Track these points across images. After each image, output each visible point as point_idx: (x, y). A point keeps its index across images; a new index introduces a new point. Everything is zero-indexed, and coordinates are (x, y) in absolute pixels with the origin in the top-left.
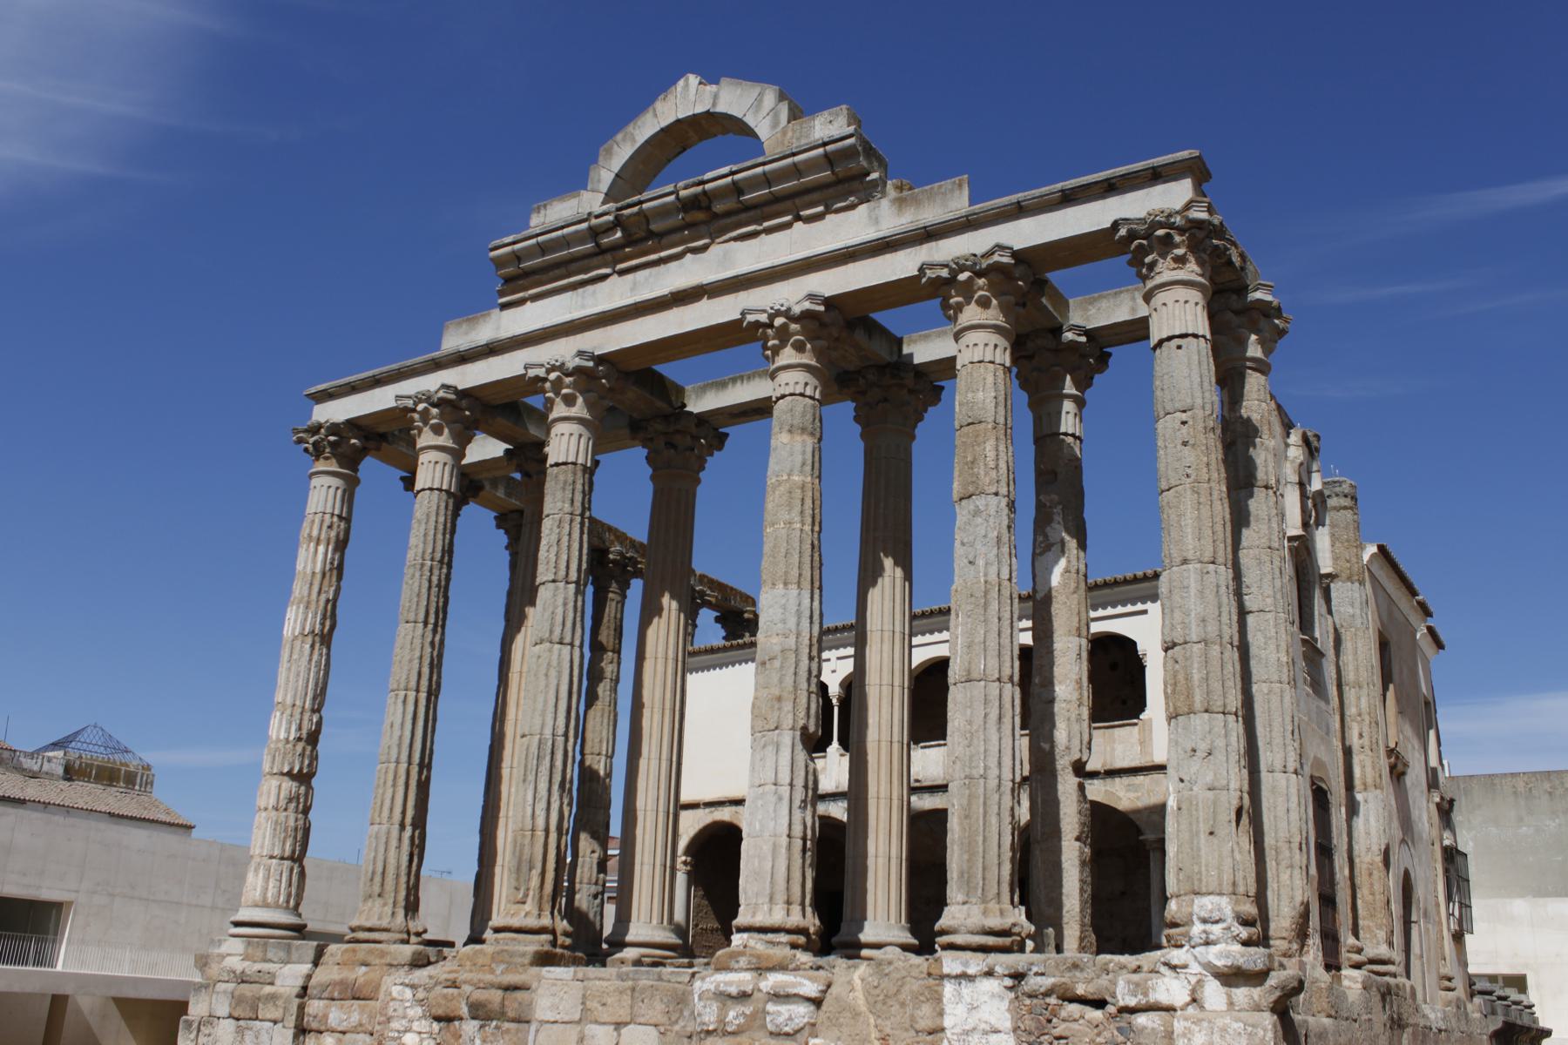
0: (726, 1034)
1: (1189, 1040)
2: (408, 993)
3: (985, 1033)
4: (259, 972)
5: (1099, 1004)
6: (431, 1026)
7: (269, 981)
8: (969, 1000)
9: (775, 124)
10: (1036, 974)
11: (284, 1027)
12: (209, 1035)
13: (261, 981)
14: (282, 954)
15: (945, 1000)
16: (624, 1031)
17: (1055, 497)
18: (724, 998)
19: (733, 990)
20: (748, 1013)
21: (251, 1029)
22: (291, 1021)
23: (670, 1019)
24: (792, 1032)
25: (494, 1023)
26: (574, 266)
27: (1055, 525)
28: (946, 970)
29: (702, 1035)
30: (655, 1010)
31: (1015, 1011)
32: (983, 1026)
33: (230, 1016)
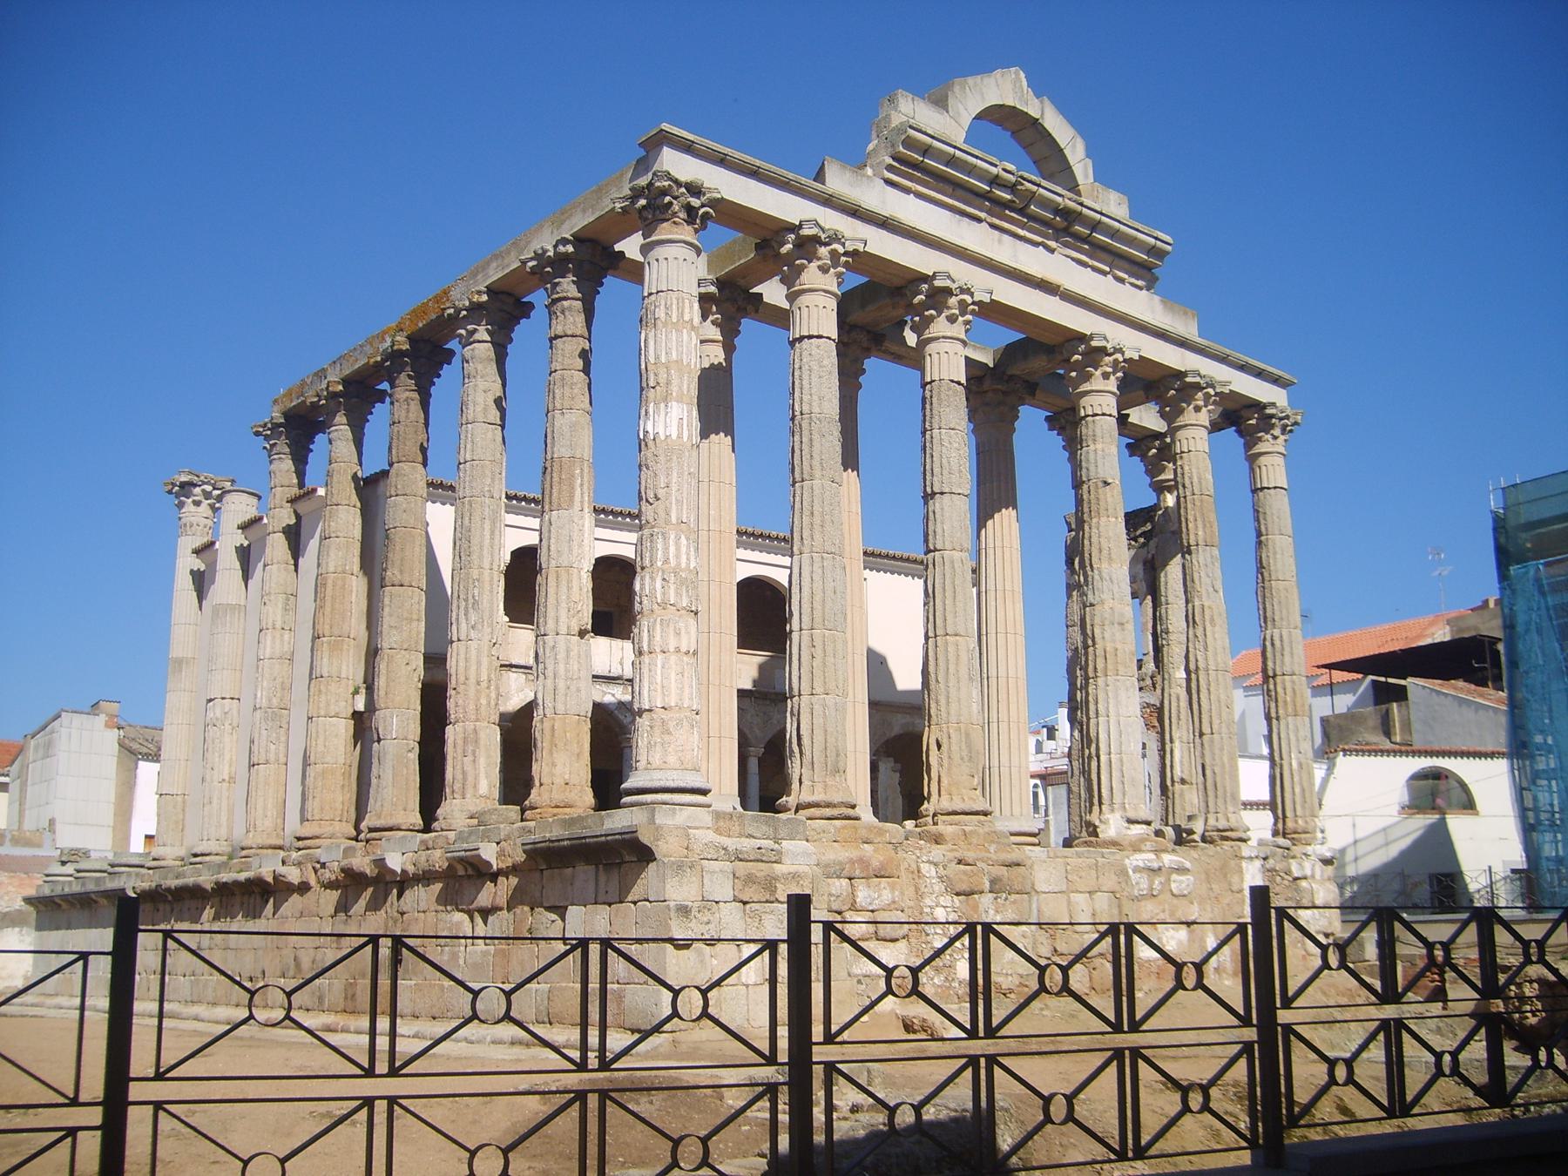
4: (759, 848)
6: (953, 901)
9: (1086, 176)
13: (764, 859)
14: (764, 828)
26: (960, 192)
28: (1244, 854)
30: (1109, 881)
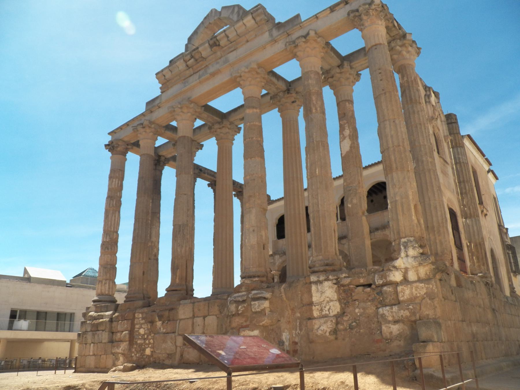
0: (239, 315)
1: (404, 293)
2: (140, 316)
3: (328, 302)
5: (369, 285)
6: (148, 326)
7: (101, 318)
8: (321, 290)
10: (345, 277)
11: (105, 332)
12: (86, 337)
15: (312, 291)
16: (206, 319)
17: (345, 121)
18: (238, 303)
19: (241, 299)
20: (245, 306)
21: (96, 334)
22: (107, 330)
23: (220, 312)
24: (260, 310)
25: (166, 322)
27: (346, 130)
28: (312, 280)
29: (231, 316)
31: (339, 293)
32: (328, 299)
33: (91, 331)
